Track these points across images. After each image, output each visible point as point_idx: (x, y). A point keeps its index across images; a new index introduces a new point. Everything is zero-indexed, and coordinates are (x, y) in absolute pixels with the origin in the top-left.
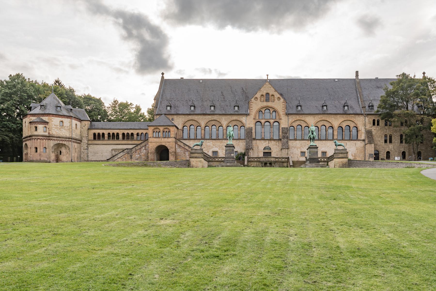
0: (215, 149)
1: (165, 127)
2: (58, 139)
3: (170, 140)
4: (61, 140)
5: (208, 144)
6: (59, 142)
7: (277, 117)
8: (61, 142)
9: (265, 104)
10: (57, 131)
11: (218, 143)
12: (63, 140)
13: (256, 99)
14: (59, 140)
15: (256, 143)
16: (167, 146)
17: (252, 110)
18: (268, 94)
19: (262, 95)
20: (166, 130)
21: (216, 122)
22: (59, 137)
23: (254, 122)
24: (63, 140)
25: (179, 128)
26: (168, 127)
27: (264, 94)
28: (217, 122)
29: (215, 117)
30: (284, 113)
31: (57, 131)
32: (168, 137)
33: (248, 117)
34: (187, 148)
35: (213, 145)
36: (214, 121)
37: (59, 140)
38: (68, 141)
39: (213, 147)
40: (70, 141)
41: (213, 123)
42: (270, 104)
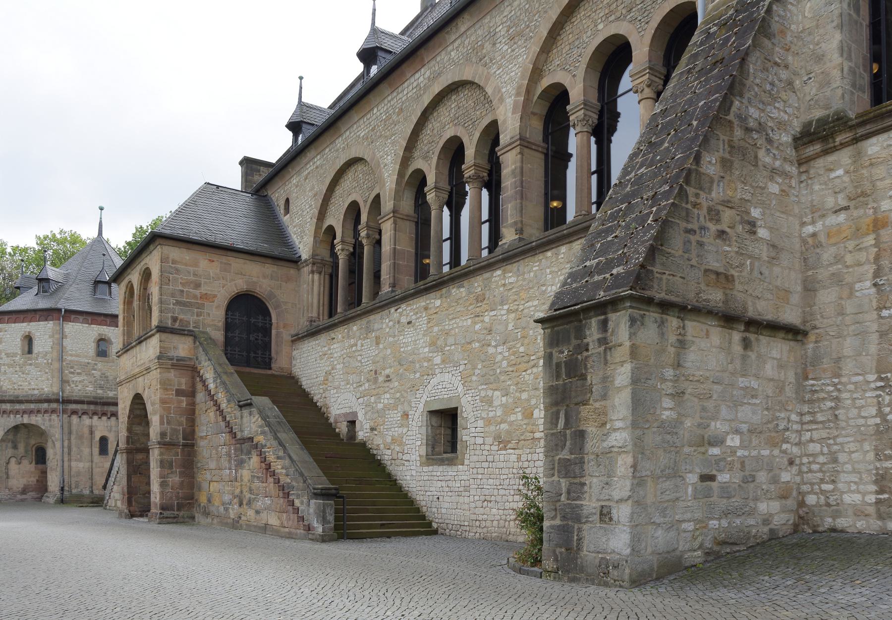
0: (445, 387)
2: (17, 406)
4: (24, 412)
6: (19, 420)
8: (26, 420)
10: (15, 378)
12: (31, 412)
14: (17, 412)
15: (861, 196)
22: (21, 402)
24: (31, 412)
25: (305, 255)
31: (15, 378)
37: (17, 412)
38: (46, 412)
39: (430, 373)
40: (53, 411)
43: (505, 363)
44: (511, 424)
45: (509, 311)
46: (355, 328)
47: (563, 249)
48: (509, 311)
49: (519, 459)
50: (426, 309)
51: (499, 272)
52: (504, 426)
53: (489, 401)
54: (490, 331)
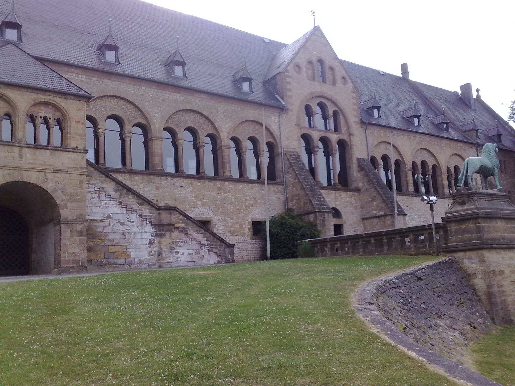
1: (43, 97)
3: (65, 159)
5: (180, 193)
7: (344, 129)
9: (318, 88)
11: (209, 190)
13: (297, 69)
16: (49, 187)
17: (291, 97)
18: (321, 62)
19: (310, 62)
20: (41, 112)
21: (198, 117)
23: (297, 134)
26: (58, 100)
27: (314, 60)
28: (202, 120)
29: (197, 102)
30: (357, 120)
32: (64, 147)
33: (284, 116)
34: (131, 201)
35: (196, 197)
36: (192, 116)
39: (195, 206)
41: (190, 120)
42: (327, 90)
43: (232, 210)
44: (235, 228)
45: (232, 196)
46: (137, 178)
47: (250, 185)
48: (232, 196)
49: (239, 238)
50: (191, 184)
51: (227, 183)
52: (232, 229)
53: (226, 221)
54: (225, 199)
